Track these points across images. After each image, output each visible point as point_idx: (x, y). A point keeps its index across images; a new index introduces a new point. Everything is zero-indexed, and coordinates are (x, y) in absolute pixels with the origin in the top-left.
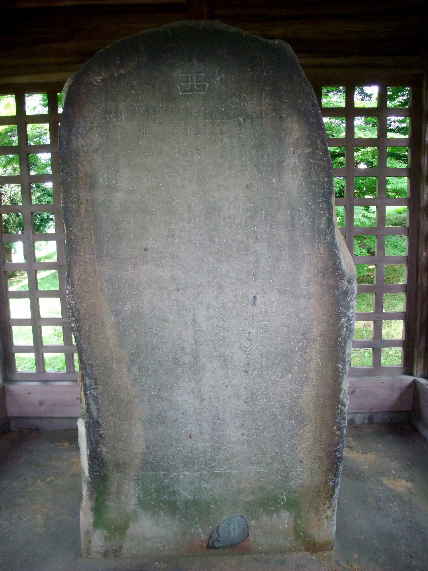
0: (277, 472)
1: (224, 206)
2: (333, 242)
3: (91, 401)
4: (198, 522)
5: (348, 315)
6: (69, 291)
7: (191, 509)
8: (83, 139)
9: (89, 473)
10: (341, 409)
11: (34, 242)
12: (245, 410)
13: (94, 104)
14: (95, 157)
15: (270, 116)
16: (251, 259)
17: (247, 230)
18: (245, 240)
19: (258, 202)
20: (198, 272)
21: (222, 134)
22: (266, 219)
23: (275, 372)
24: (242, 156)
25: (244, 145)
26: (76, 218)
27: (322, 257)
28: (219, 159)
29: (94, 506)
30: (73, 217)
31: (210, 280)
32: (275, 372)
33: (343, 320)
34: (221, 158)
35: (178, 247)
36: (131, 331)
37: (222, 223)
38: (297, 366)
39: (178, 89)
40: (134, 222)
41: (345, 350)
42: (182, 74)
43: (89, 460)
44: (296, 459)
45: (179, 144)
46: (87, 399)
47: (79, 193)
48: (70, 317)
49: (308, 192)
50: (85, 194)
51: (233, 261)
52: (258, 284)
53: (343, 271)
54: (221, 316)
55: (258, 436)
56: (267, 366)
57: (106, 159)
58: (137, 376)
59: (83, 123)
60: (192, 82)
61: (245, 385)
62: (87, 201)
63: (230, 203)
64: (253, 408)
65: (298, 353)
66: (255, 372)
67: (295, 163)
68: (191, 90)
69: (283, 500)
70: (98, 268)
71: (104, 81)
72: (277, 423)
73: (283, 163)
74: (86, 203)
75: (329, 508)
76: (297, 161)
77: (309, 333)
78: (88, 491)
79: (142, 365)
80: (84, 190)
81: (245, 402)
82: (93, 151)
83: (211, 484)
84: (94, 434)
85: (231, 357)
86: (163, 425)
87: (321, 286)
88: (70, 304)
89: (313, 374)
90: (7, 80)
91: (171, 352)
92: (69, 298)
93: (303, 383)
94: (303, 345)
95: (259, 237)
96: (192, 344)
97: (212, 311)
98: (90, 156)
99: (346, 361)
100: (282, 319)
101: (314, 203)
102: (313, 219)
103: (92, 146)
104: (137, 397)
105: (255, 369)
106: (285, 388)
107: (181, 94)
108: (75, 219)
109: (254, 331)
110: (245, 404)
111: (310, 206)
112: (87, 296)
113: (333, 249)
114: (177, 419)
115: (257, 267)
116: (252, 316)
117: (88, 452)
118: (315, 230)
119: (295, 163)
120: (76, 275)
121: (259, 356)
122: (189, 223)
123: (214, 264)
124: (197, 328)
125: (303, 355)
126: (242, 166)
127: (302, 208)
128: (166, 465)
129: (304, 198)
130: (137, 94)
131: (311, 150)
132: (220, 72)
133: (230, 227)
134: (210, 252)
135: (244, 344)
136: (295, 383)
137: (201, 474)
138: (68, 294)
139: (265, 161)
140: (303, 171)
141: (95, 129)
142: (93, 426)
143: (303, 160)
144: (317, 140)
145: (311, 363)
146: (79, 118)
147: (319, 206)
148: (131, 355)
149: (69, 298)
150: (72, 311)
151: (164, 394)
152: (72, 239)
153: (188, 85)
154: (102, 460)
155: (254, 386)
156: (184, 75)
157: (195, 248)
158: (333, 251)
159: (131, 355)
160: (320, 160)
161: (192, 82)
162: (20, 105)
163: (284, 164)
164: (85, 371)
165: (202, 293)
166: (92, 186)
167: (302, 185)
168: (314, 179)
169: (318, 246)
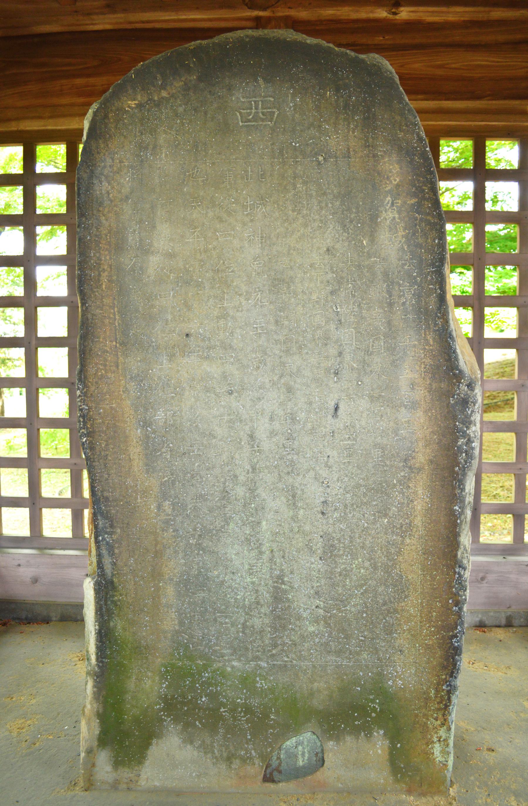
0: (366, 666)
1: (296, 277)
2: (447, 330)
3: (104, 552)
4: (250, 740)
5: (469, 435)
6: (81, 392)
7: (239, 720)
8: (109, 183)
9: (97, 659)
10: (459, 573)
11: (37, 349)
12: (321, 570)
13: (125, 137)
14: (124, 207)
15: (360, 154)
16: (333, 351)
17: (327, 310)
18: (324, 324)
19: (342, 271)
20: (258, 368)
21: (295, 178)
22: (354, 296)
23: (364, 515)
24: (321, 208)
25: (325, 194)
26: (95, 290)
27: (431, 350)
28: (290, 212)
29: (101, 711)
30: (92, 289)
31: (275, 379)
32: (364, 515)
33: (461, 441)
34: (293, 211)
35: (232, 333)
36: (164, 450)
37: (293, 300)
38: (396, 507)
39: (237, 119)
40: (174, 296)
41: (464, 486)
42: (243, 97)
43: (97, 640)
44: (394, 647)
45: (237, 192)
46: (98, 548)
47: (100, 255)
48: (81, 428)
49: (411, 259)
50: (108, 258)
51: (307, 353)
52: (342, 386)
53: (461, 371)
54: (289, 431)
55: (339, 610)
56: (353, 505)
57: (138, 210)
58: (169, 515)
59: (109, 162)
60: (256, 108)
61: (322, 533)
62: (110, 266)
63: (305, 273)
64: (332, 568)
65: (397, 487)
66: (336, 515)
67: (394, 218)
68: (255, 119)
69: (374, 710)
70: (121, 359)
71: (140, 106)
72: (366, 591)
73: (377, 219)
74: (109, 269)
75: (443, 724)
76: (397, 216)
77: (413, 458)
78: (94, 686)
79: (177, 500)
80: (107, 253)
81: (320, 558)
82: (121, 200)
83: (270, 681)
84: (106, 601)
85: (302, 490)
86: (203, 590)
87: (429, 392)
88: (81, 410)
89: (419, 518)
90: (13, 127)
91: (218, 481)
92: (80, 401)
93: (403, 532)
94: (405, 477)
95: (343, 321)
96: (248, 470)
97: (277, 425)
98: (116, 206)
99: (466, 503)
100: (375, 438)
101: (420, 274)
102: (418, 296)
103: (120, 192)
104: (169, 547)
105: (336, 509)
106: (378, 538)
107: (241, 124)
108: (95, 292)
109: (335, 453)
110: (320, 562)
111: (415, 278)
112: (105, 399)
113: (447, 339)
114: (222, 582)
115: (340, 363)
116: (333, 432)
117: (97, 627)
118: (421, 312)
119: (394, 218)
120: (91, 370)
121: (341, 490)
122: (247, 299)
123: (281, 357)
124: (256, 448)
125: (404, 490)
126: (321, 221)
127: (403, 281)
128: (207, 650)
129: (406, 267)
130: (183, 124)
131: (417, 200)
132: (294, 95)
133: (303, 306)
134: (275, 341)
135: (321, 472)
136: (393, 532)
137: (257, 665)
138: (80, 396)
139: (353, 216)
140: (405, 229)
141: (125, 171)
142: (105, 589)
143: (404, 214)
144: (424, 188)
145: (415, 503)
146: (104, 155)
147: (426, 277)
148: (162, 484)
149: (80, 401)
150: (84, 419)
151: (206, 543)
152: (87, 319)
153: (251, 113)
154: (116, 640)
155: (334, 535)
156: (248, 98)
157: (256, 335)
158: (447, 341)
159: (162, 484)
160: (428, 214)
161: (256, 108)
162: (30, 159)
163: (379, 220)
164: (97, 507)
165: (263, 398)
166: (119, 247)
167: (403, 248)
168: (420, 240)
169: (425, 334)
